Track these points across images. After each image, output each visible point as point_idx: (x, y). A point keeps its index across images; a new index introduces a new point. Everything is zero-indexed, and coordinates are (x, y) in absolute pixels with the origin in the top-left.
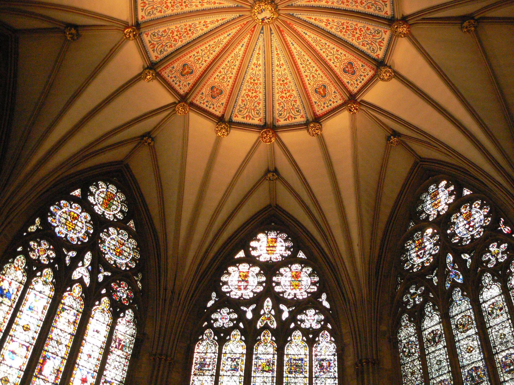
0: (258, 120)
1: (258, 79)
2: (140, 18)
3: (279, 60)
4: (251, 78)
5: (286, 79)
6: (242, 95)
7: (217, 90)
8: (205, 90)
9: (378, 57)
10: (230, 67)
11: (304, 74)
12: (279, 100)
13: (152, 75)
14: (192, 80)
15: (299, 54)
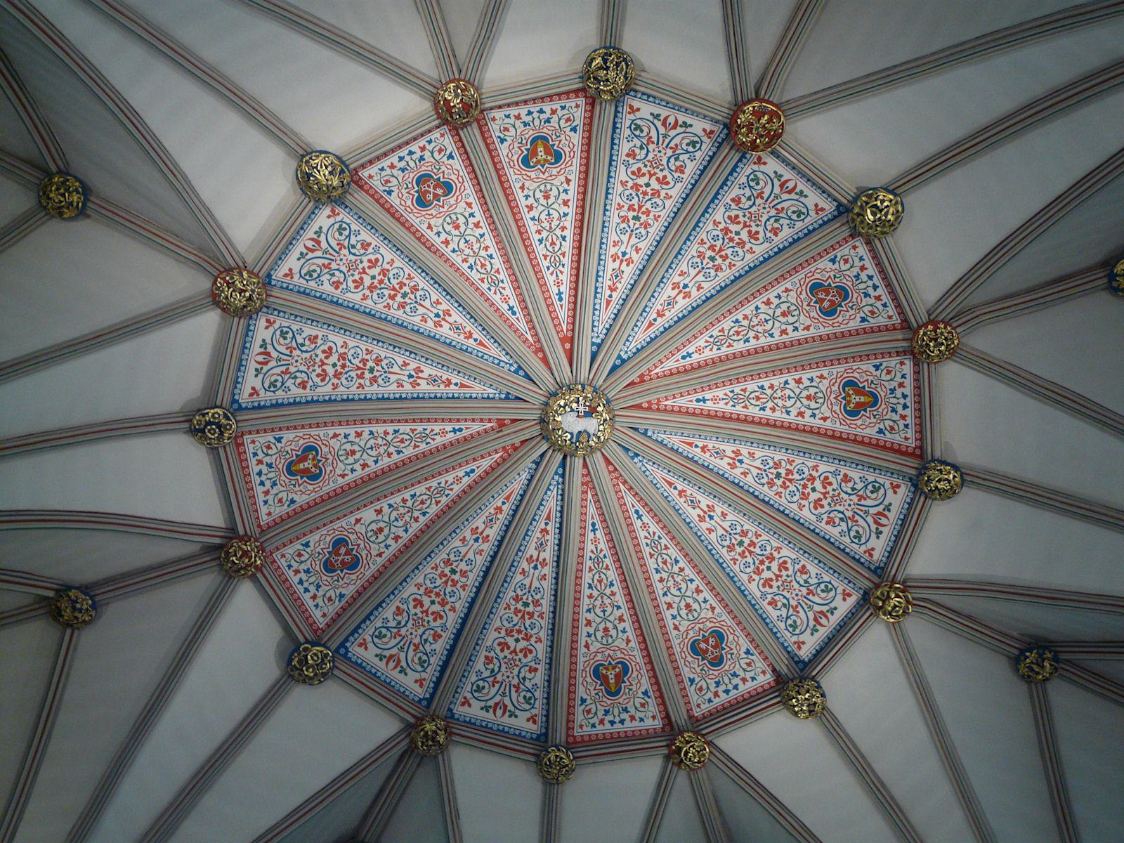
0: (765, 163)
1: (701, 255)
2: (852, 601)
3: (618, 274)
4: (718, 268)
5: (624, 219)
6: (766, 245)
7: (822, 301)
8: (852, 324)
9: (333, 211)
10: (751, 327)
11: (571, 210)
12: (677, 180)
13: (929, 480)
14: (864, 367)
15: (556, 265)
